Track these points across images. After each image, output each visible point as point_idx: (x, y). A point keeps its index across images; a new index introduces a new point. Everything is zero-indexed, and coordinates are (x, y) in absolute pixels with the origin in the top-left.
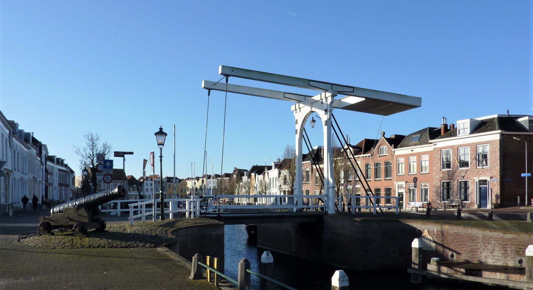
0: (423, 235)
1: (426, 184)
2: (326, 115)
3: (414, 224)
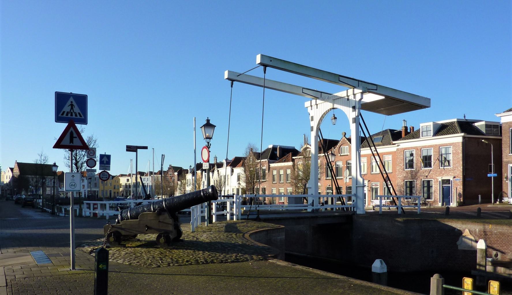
0: (464, 235)
1: (377, 184)
2: (355, 112)
3: (452, 224)
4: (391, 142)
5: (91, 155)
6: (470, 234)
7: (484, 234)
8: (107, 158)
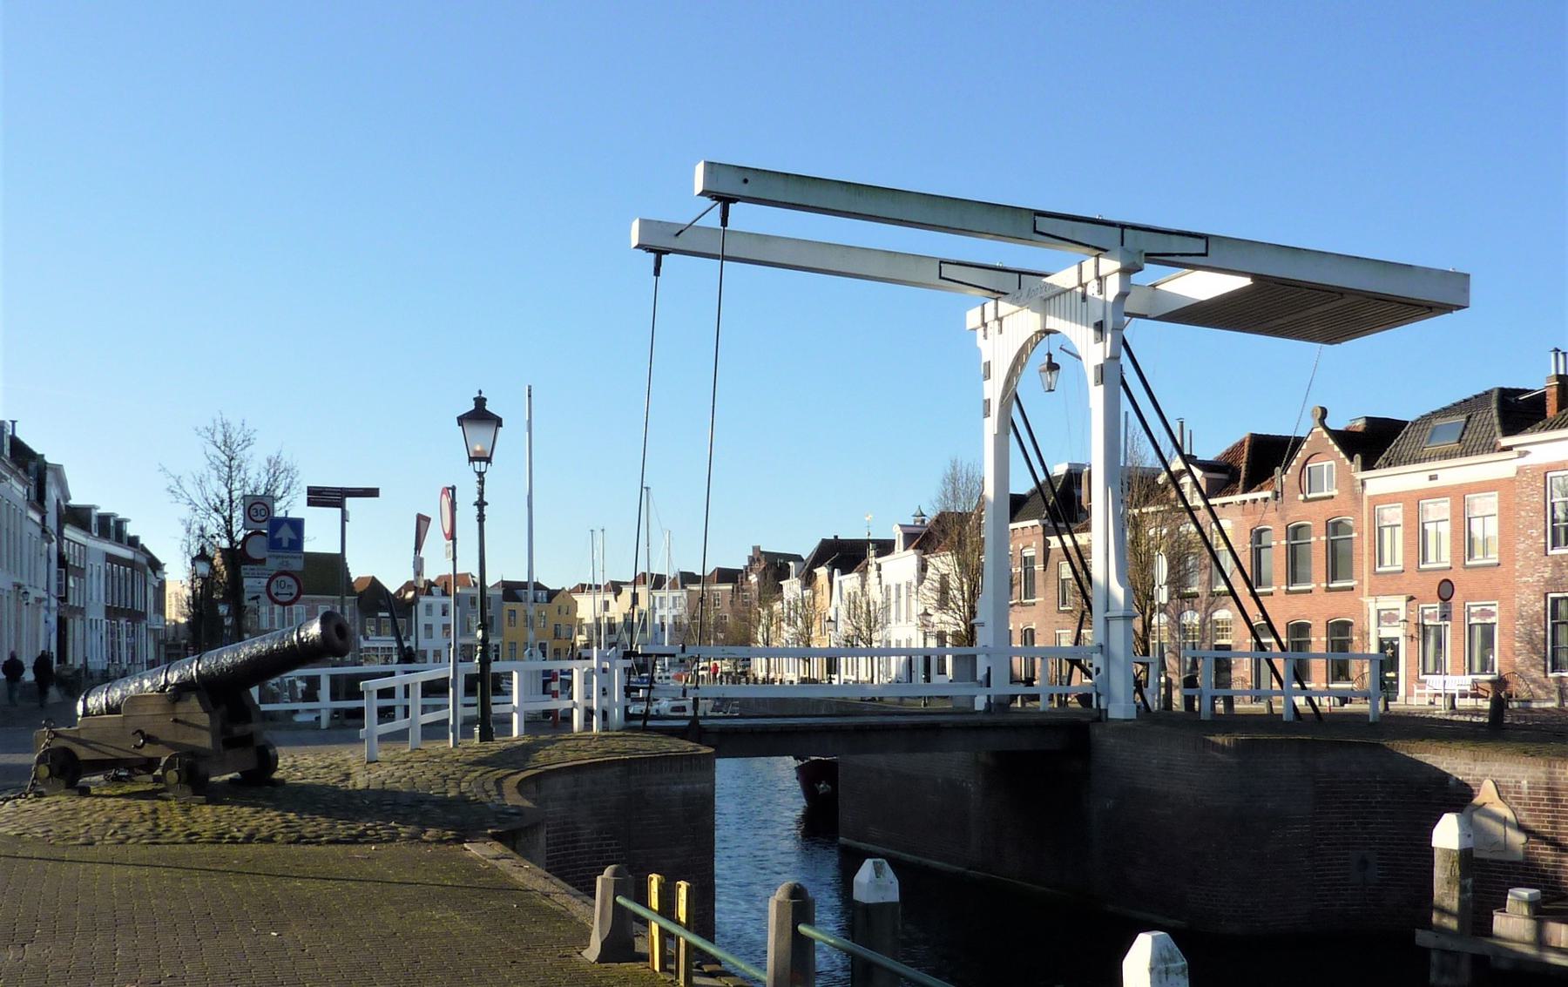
0: (1477, 801)
1: (1488, 608)
2: (1102, 343)
3: (1440, 758)
4: (1494, 440)
5: (257, 522)
6: (1500, 797)
7: (1548, 799)
8: (291, 528)
